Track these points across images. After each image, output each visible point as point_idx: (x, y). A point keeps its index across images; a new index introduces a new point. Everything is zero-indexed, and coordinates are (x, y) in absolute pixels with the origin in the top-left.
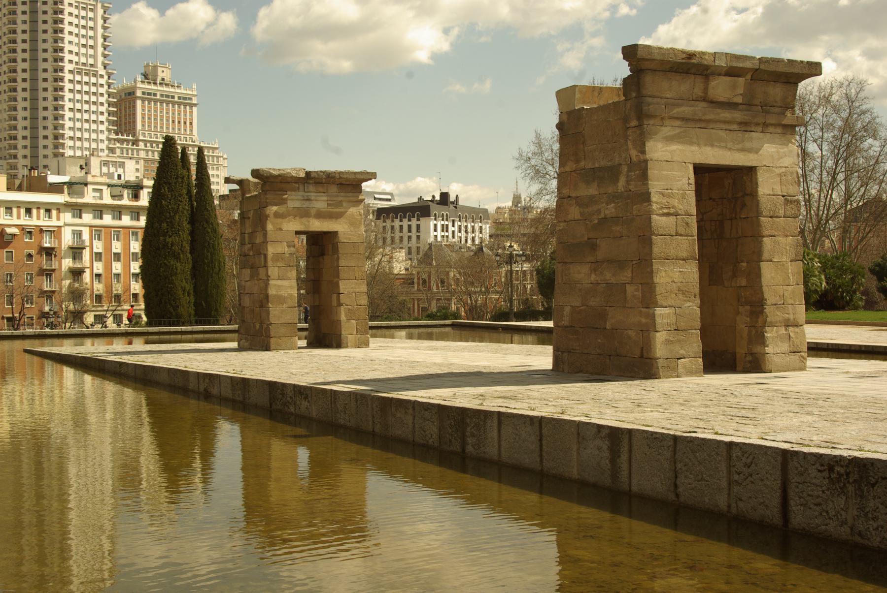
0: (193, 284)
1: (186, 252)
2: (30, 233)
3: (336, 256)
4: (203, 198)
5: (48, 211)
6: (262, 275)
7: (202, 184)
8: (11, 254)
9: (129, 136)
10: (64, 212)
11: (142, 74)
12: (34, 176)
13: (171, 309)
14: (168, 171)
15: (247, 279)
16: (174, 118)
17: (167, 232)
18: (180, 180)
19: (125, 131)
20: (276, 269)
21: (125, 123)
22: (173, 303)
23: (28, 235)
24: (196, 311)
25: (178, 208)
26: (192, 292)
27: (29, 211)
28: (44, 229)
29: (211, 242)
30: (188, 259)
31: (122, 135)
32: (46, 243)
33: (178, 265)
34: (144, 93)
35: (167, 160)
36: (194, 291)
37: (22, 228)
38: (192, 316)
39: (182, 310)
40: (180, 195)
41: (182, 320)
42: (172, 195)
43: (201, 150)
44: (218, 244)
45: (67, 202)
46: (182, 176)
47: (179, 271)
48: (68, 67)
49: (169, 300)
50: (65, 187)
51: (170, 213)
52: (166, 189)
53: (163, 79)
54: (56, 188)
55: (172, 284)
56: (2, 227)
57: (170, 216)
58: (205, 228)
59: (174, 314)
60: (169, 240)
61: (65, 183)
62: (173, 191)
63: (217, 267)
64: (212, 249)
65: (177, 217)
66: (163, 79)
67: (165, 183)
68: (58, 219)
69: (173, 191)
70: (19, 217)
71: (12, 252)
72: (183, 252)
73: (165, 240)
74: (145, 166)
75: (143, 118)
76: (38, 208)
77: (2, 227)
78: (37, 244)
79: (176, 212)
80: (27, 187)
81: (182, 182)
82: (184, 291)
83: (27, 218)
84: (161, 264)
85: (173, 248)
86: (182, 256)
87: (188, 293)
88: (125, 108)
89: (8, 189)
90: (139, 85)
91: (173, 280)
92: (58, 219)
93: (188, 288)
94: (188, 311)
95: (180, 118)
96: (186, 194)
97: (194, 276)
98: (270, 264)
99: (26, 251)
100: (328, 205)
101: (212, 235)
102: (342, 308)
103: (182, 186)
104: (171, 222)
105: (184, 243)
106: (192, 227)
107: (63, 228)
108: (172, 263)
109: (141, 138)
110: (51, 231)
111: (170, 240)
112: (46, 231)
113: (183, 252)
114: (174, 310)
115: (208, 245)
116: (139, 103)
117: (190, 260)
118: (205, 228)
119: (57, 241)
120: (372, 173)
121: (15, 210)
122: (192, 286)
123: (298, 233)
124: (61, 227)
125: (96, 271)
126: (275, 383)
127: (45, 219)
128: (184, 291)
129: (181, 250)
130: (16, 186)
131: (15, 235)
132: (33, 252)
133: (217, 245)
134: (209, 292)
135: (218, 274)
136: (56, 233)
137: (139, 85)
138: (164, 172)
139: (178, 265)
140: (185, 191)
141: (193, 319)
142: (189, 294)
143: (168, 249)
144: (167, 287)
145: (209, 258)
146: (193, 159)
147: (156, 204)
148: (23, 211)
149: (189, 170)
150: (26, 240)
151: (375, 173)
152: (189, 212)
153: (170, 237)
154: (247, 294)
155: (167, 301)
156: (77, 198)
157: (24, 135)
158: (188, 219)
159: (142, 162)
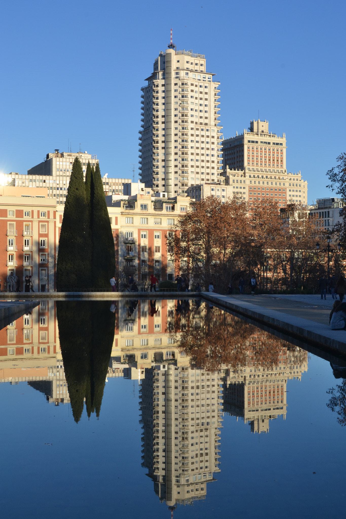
11: (249, 129)
16: (270, 157)
19: (237, 167)
21: (237, 162)
31: (235, 170)
34: (249, 141)
48: (190, 125)
53: (263, 132)
61: (122, 200)
66: (263, 132)
74: (249, 191)
75: (249, 158)
88: (237, 152)
95: (274, 158)
137: (246, 136)
159: (247, 188)
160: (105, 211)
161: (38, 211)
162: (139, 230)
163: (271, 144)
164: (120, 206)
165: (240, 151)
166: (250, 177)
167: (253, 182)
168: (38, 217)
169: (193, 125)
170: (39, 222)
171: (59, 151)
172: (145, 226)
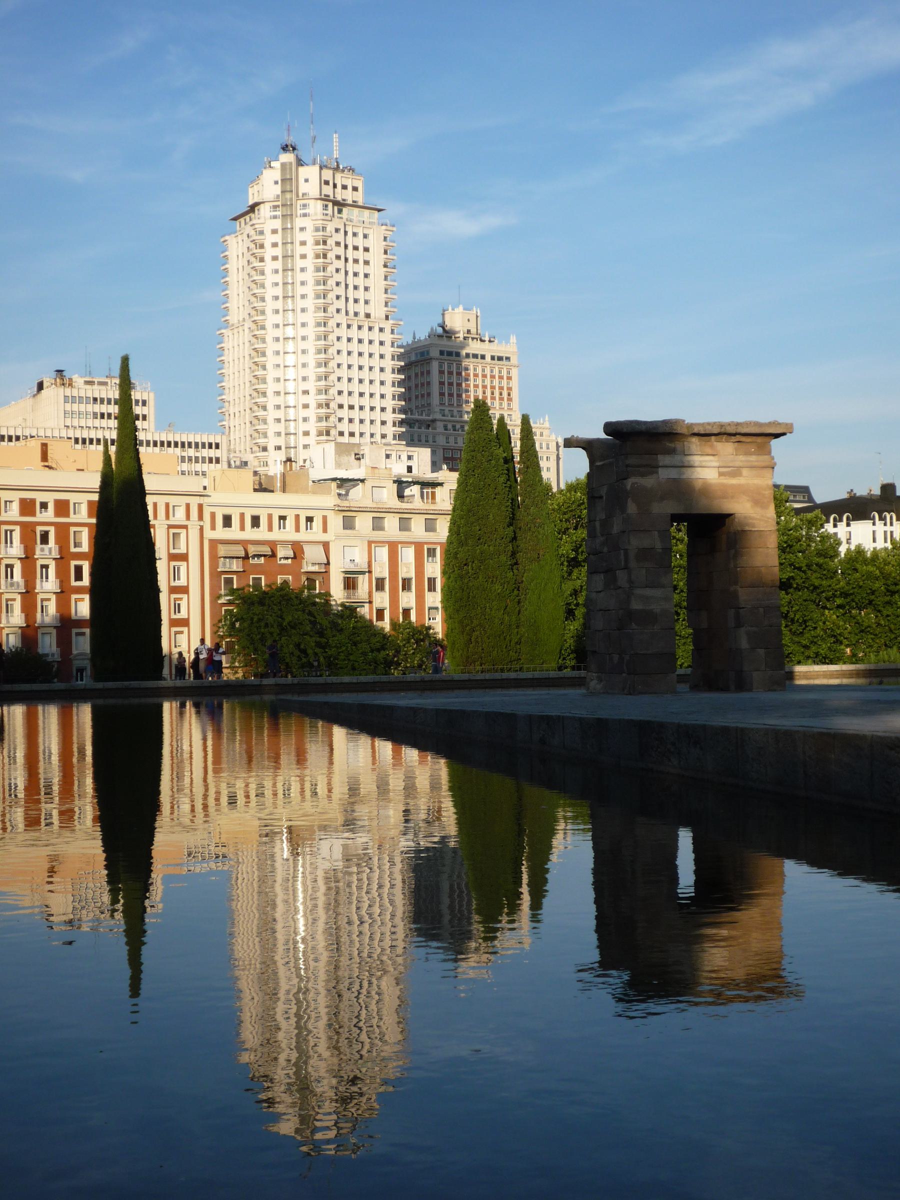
3: (733, 551)
6: (622, 577)
9: (422, 415)
15: (600, 590)
20: (644, 571)
21: (417, 397)
34: (442, 353)
53: (469, 332)
66: (469, 332)
68: (325, 530)
75: (441, 388)
88: (416, 375)
90: (437, 341)
92: (325, 530)
98: (633, 564)
100: (721, 474)
102: (743, 630)
109: (438, 416)
116: (435, 365)
120: (787, 424)
123: (677, 518)
125: (377, 604)
126: (648, 722)
151: (792, 425)
154: (601, 610)
157: (274, 241)
160: (463, 504)
161: (167, 505)
162: (370, 543)
163: (488, 358)
165: (422, 373)
166: (446, 428)
167: (452, 439)
168: (167, 517)
169: (341, 318)
170: (170, 527)
171: (64, 373)
172: (378, 535)
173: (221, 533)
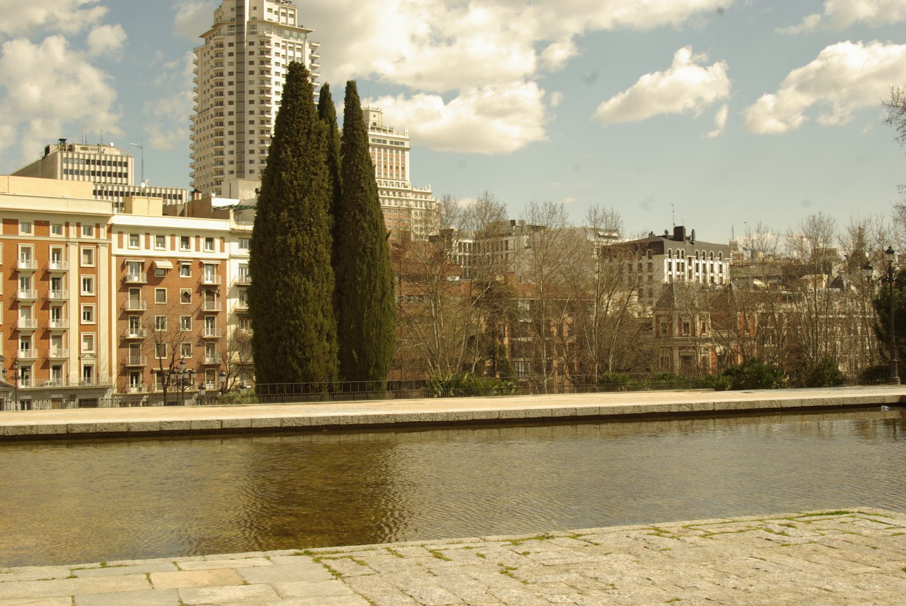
0: (337, 320)
1: (325, 262)
2: (187, 267)
4: (355, 168)
5: (210, 240)
7: (353, 144)
8: (163, 292)
10: (229, 242)
12: (198, 201)
13: (295, 365)
14: (292, 122)
17: (290, 227)
18: (313, 136)
22: (299, 353)
23: (185, 269)
24: (341, 367)
25: (311, 186)
26: (335, 334)
27: (185, 240)
28: (204, 262)
29: (369, 245)
30: (328, 274)
32: (207, 279)
33: (310, 285)
35: (292, 102)
36: (338, 333)
37: (177, 261)
38: (335, 377)
39: (316, 365)
40: (315, 163)
41: (316, 384)
42: (299, 163)
43: (351, 88)
44: (382, 250)
45: (233, 229)
46: (317, 131)
47: (311, 295)
49: (291, 349)
50: (231, 211)
51: (295, 194)
52: (289, 153)
54: (221, 213)
55: (298, 319)
56: (152, 260)
57: (296, 199)
58: (359, 221)
59: (300, 372)
60: (292, 241)
61: (231, 207)
62: (301, 155)
63: (378, 289)
64: (370, 258)
65: (306, 199)
67: (288, 142)
68: (222, 250)
69: (301, 155)
70: (173, 248)
71: (164, 290)
72: (318, 261)
73: (286, 240)
76: (198, 237)
77: (152, 260)
78: (196, 280)
79: (306, 193)
80: (188, 214)
81: (318, 140)
82: (320, 332)
83: (184, 249)
84: (277, 284)
85: (300, 254)
86: (316, 269)
87: (328, 335)
89: (164, 215)
91: (300, 313)
92: (222, 250)
93: (327, 327)
94: (327, 369)
96: (326, 163)
97: (340, 305)
99: (182, 290)
101: (370, 233)
103: (318, 148)
104: (297, 210)
105: (320, 247)
106: (336, 219)
107: (228, 262)
108: (297, 280)
110: (213, 265)
111: (293, 240)
112: (207, 265)
113: (318, 261)
114: (301, 366)
115: (364, 250)
117: (332, 278)
118: (359, 221)
119: (220, 277)
121: (168, 239)
122: (336, 323)
124: (225, 260)
127: (206, 250)
128: (320, 332)
129: (315, 258)
130: (179, 212)
131: (168, 269)
132: (190, 290)
133: (378, 252)
134: (365, 334)
135: (381, 300)
136: (219, 267)
138: (286, 124)
139: (310, 285)
140: (323, 157)
141: (336, 381)
142: (329, 338)
143: (291, 256)
144: (289, 324)
145: (365, 273)
146: (340, 109)
147: (272, 180)
148: (178, 240)
149: (332, 122)
150: (181, 276)
152: (331, 193)
153: (294, 235)
155: (288, 350)
156: (246, 224)
158: (328, 205)
164: (227, 217)
173: (128, 250)
